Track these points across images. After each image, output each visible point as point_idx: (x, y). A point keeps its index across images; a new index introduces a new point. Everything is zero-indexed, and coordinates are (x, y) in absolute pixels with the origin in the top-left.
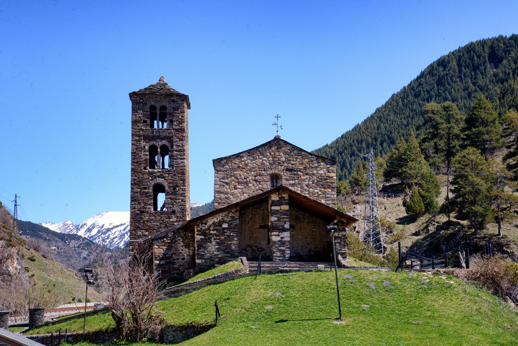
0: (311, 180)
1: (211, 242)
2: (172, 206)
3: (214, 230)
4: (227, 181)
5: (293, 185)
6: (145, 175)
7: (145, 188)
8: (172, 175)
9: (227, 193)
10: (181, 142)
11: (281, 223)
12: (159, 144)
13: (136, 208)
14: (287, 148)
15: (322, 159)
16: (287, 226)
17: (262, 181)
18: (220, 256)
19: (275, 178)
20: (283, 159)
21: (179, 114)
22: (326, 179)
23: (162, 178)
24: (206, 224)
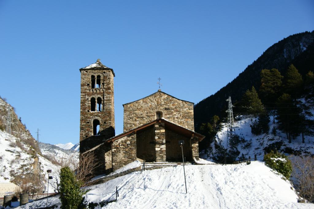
0: (179, 115)
1: (120, 152)
3: (122, 145)
4: (131, 117)
5: (169, 118)
7: (88, 123)
8: (103, 114)
9: (131, 124)
10: (109, 95)
11: (161, 140)
12: (96, 97)
13: (83, 134)
14: (165, 97)
15: (185, 103)
16: (164, 141)
17: (151, 116)
18: (125, 160)
19: (159, 114)
20: (163, 103)
21: (107, 79)
22: (188, 114)
23: (98, 116)
24: (117, 142)
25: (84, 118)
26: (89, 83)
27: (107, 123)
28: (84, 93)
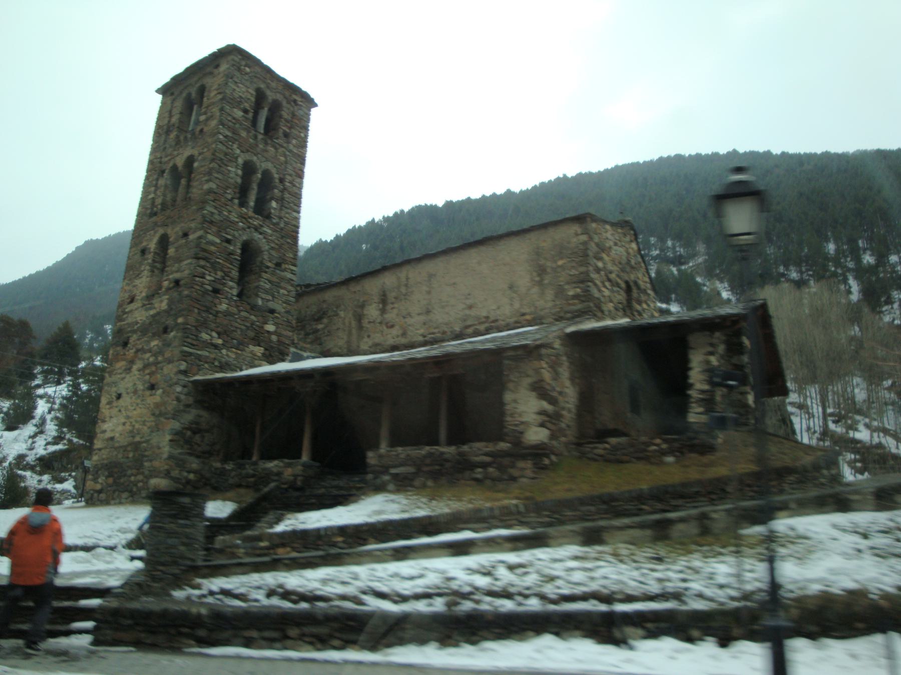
2: (270, 298)
6: (233, 214)
23: (261, 233)
25: (217, 217)
26: (247, 106)
27: (285, 270)
28: (229, 128)
